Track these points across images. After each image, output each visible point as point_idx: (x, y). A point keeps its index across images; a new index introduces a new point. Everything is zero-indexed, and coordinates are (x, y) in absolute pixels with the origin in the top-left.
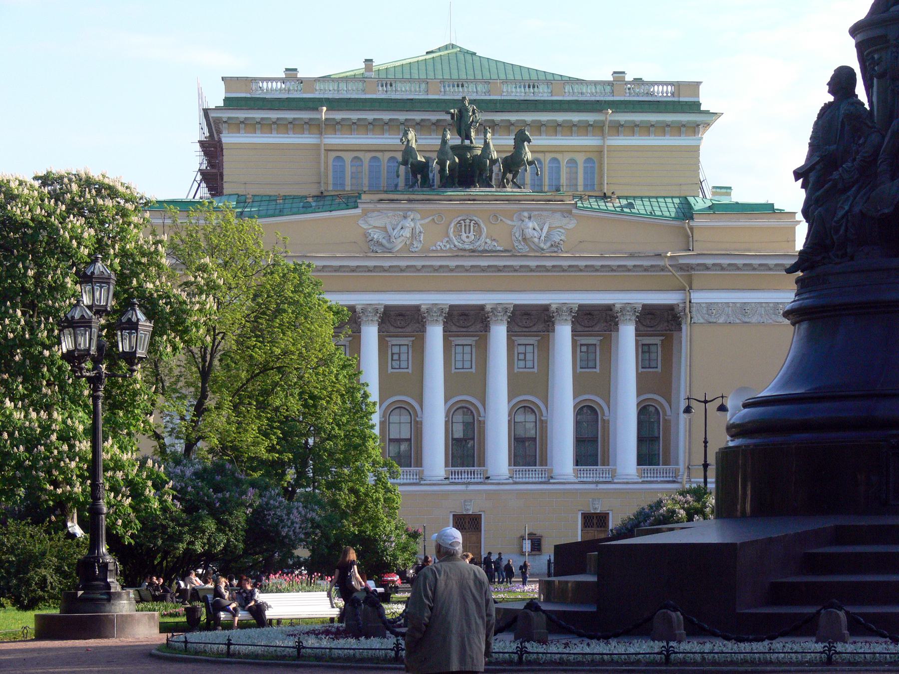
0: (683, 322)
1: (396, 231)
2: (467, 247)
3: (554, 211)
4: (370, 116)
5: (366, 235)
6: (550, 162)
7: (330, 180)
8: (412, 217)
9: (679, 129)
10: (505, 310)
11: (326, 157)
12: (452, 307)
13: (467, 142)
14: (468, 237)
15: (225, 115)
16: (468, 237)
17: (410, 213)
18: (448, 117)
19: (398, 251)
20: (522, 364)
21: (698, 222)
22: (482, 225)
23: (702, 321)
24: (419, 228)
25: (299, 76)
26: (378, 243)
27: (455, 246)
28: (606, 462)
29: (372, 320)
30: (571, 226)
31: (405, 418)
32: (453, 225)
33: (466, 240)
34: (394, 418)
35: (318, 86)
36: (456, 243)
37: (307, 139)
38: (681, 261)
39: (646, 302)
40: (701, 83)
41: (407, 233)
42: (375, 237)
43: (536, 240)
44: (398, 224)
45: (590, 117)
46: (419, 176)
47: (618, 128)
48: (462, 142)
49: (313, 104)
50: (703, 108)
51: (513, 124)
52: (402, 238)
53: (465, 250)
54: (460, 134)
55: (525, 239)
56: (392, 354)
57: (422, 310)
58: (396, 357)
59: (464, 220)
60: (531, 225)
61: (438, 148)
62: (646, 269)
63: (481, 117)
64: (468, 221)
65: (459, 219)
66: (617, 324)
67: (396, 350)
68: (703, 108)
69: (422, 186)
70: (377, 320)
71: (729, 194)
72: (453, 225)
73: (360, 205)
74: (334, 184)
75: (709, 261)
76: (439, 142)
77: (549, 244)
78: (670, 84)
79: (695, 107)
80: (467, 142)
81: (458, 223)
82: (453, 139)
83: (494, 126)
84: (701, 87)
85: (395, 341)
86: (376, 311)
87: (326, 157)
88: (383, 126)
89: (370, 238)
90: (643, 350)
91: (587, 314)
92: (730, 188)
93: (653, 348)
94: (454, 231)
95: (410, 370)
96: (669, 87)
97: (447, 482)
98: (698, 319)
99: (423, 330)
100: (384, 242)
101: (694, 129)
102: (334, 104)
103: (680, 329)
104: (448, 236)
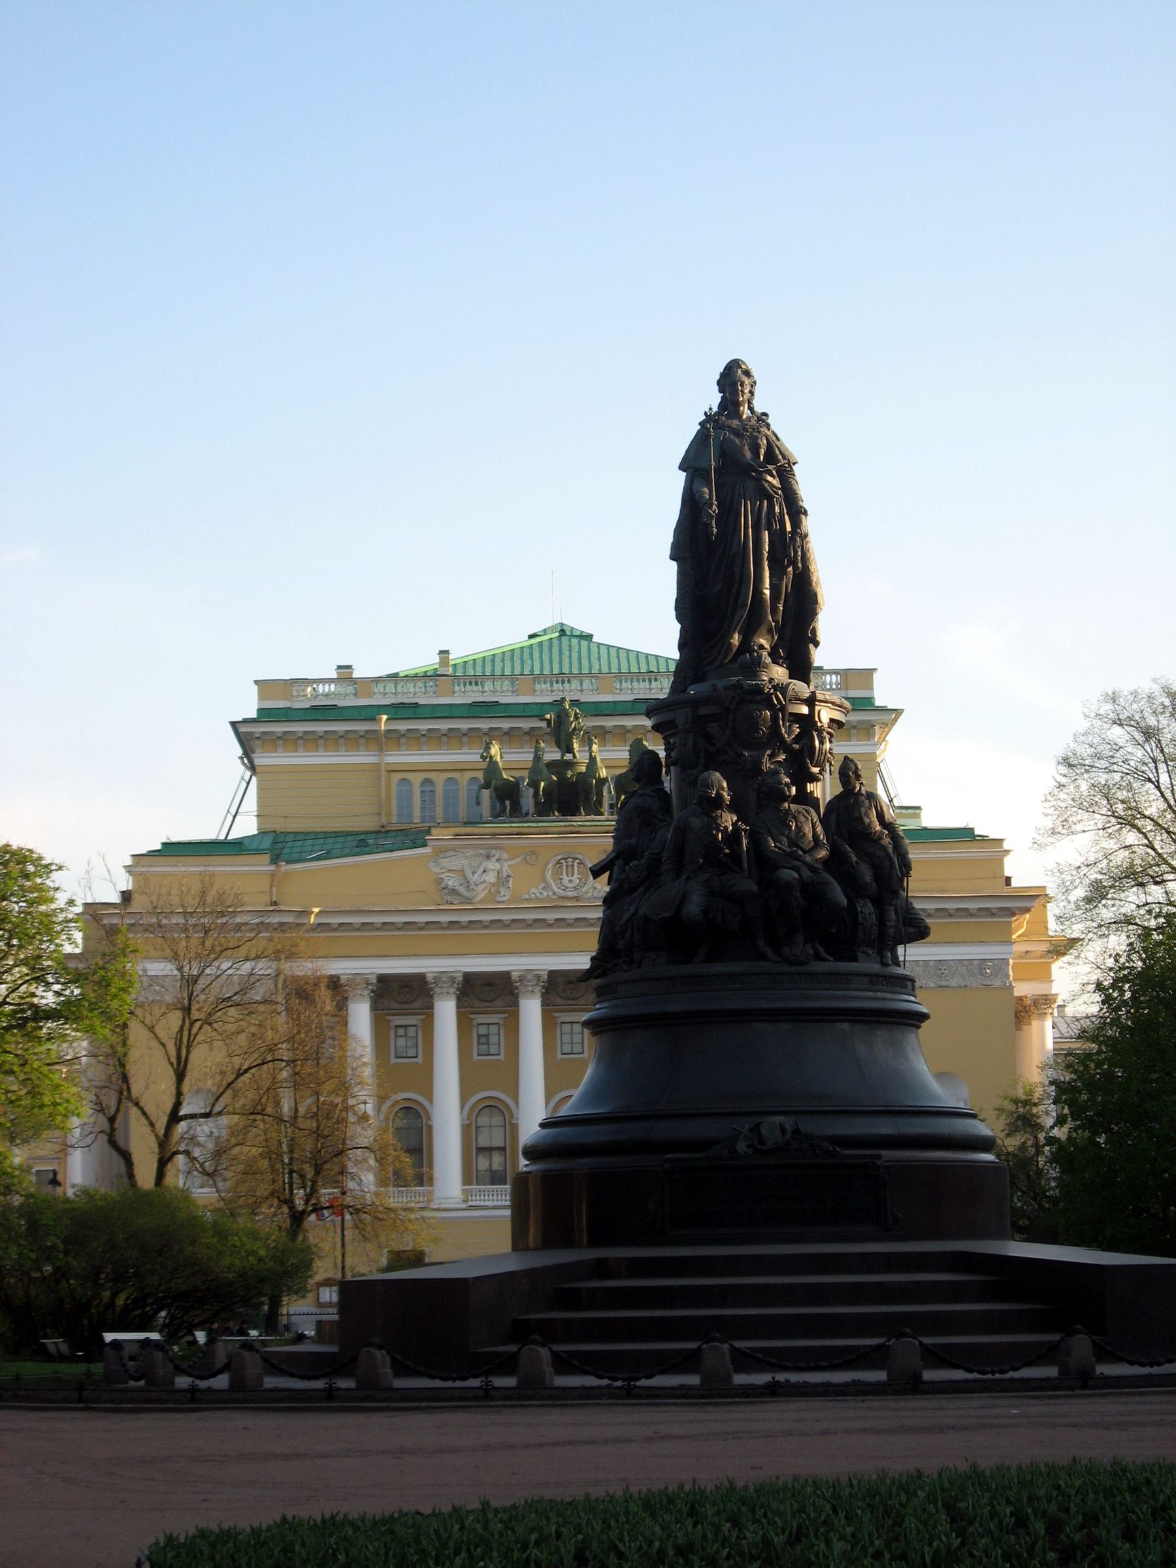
1: (476, 876)
2: (570, 894)
4: (444, 725)
5: (439, 881)
6: (398, 785)
7: (394, 811)
8: (497, 856)
11: (388, 780)
12: (552, 974)
13: (568, 757)
14: (570, 881)
15: (258, 729)
16: (570, 881)
17: (493, 852)
18: (544, 724)
19: (479, 902)
24: (506, 870)
25: (354, 676)
26: (454, 892)
27: (554, 893)
29: (447, 993)
31: (497, 1120)
32: (550, 866)
33: (569, 885)
34: (484, 1120)
35: (379, 688)
36: (556, 890)
37: (363, 758)
41: (491, 878)
42: (450, 883)
44: (479, 866)
46: (508, 803)
48: (562, 757)
49: (369, 714)
50: (878, 703)
51: (629, 731)
52: (483, 886)
54: (558, 745)
56: (479, 1036)
57: (513, 978)
59: (565, 859)
61: (529, 765)
63: (588, 723)
65: (559, 857)
67: (483, 1030)
68: (878, 703)
69: (511, 816)
70: (454, 993)
71: (918, 816)
72: (550, 866)
73: (429, 843)
74: (400, 815)
76: (531, 757)
78: (834, 673)
80: (568, 757)
81: (558, 863)
82: (552, 754)
83: (603, 734)
84: (876, 676)
85: (483, 1019)
86: (453, 979)
87: (388, 780)
88: (461, 737)
89: (443, 885)
92: (919, 808)
94: (553, 873)
95: (502, 1057)
96: (834, 677)
99: (515, 1004)
100: (462, 890)
101: (867, 730)
102: (400, 711)
104: (544, 879)
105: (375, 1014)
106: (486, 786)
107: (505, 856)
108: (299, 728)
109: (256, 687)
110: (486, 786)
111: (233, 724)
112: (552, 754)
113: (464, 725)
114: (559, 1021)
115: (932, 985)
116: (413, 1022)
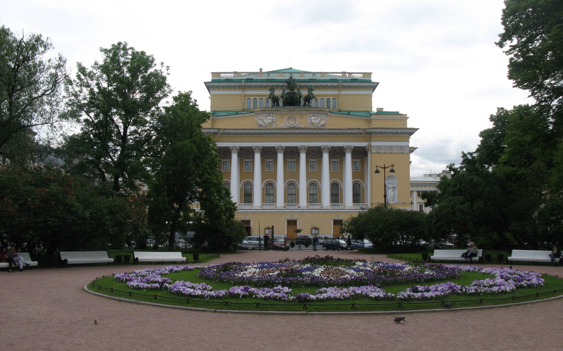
0: (368, 152)
3: (322, 114)
4: (259, 84)
9: (366, 88)
10: (305, 148)
13: (292, 91)
17: (271, 115)
20: (312, 168)
21: (373, 117)
22: (297, 119)
23: (375, 152)
26: (261, 125)
28: (342, 202)
30: (327, 119)
38: (367, 131)
39: (355, 145)
40: (371, 73)
43: (316, 124)
45: (335, 84)
46: (276, 103)
47: (344, 88)
48: (291, 91)
49: (239, 81)
53: (291, 127)
54: (289, 89)
55: (312, 123)
58: (268, 166)
60: (313, 118)
62: (355, 134)
64: (292, 117)
66: (345, 155)
72: (286, 118)
75: (377, 131)
77: (320, 125)
79: (370, 81)
80: (292, 91)
81: (289, 118)
84: (372, 75)
90: (354, 163)
91: (334, 151)
93: (358, 163)
97: (284, 208)
98: (374, 151)
100: (263, 124)
102: (248, 80)
103: (367, 156)
104: (285, 122)
105: (240, 159)
106: (270, 98)
107: (274, 115)
108: (222, 84)
109: (211, 75)
110: (270, 98)
111: (205, 83)
112: (287, 91)
113: (265, 84)
114: (288, 161)
115: (388, 152)
116: (250, 161)
